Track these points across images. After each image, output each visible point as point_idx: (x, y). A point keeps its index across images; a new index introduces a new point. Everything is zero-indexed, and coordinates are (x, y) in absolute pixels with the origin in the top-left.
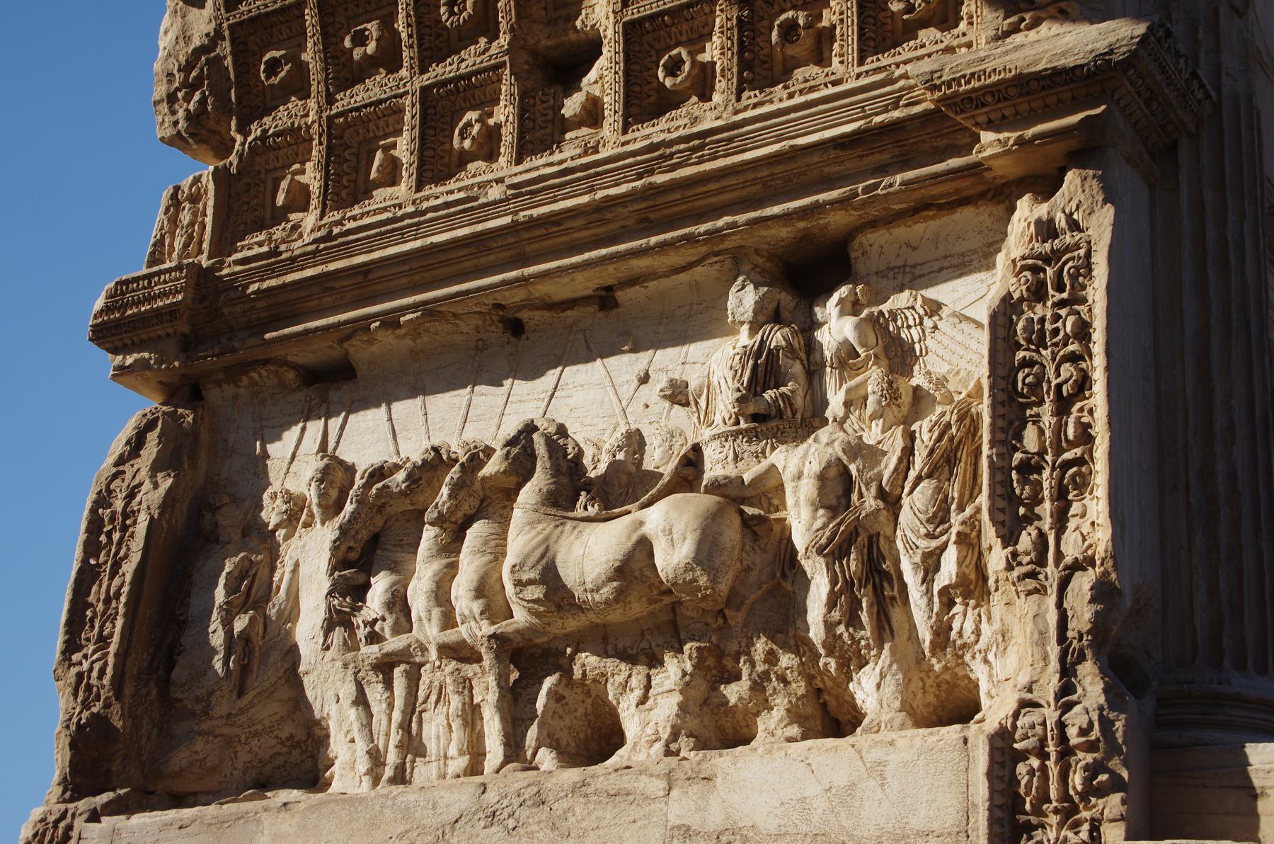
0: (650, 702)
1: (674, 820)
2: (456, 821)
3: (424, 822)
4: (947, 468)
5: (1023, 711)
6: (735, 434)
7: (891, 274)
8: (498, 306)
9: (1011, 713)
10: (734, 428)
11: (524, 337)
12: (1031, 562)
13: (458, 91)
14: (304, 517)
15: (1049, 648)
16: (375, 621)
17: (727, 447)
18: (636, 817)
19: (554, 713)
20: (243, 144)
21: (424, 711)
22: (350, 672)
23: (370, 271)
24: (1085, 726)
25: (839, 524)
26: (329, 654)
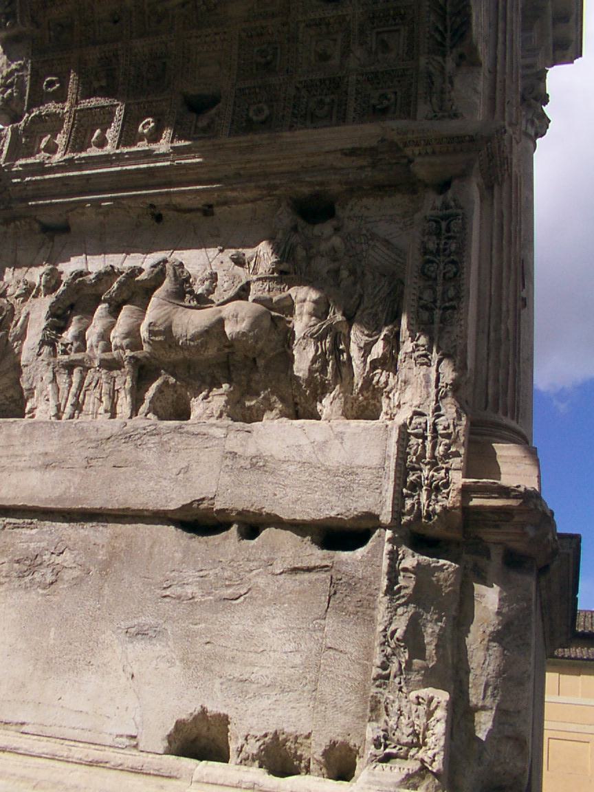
0: (210, 399)
1: (228, 449)
2: (109, 438)
3: (92, 437)
4: (381, 306)
5: (414, 417)
6: (271, 279)
7: (355, 219)
8: (152, 206)
9: (409, 417)
10: (271, 276)
11: (161, 223)
12: (425, 350)
13: (145, 108)
14: (34, 293)
15: (430, 390)
16: (68, 344)
17: (265, 284)
18: (208, 446)
19: (158, 398)
20: (28, 118)
21: (88, 390)
22: (51, 367)
23: (91, 179)
24: (446, 426)
25: (323, 325)
26: (40, 358)
